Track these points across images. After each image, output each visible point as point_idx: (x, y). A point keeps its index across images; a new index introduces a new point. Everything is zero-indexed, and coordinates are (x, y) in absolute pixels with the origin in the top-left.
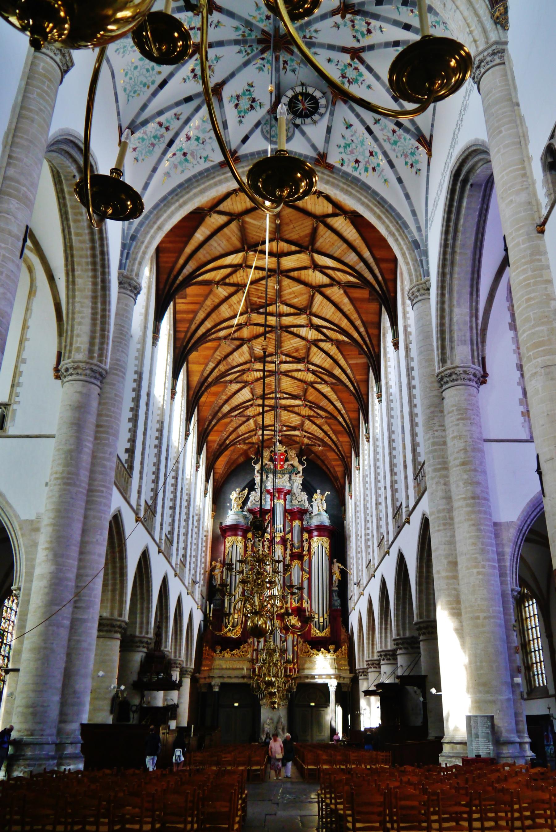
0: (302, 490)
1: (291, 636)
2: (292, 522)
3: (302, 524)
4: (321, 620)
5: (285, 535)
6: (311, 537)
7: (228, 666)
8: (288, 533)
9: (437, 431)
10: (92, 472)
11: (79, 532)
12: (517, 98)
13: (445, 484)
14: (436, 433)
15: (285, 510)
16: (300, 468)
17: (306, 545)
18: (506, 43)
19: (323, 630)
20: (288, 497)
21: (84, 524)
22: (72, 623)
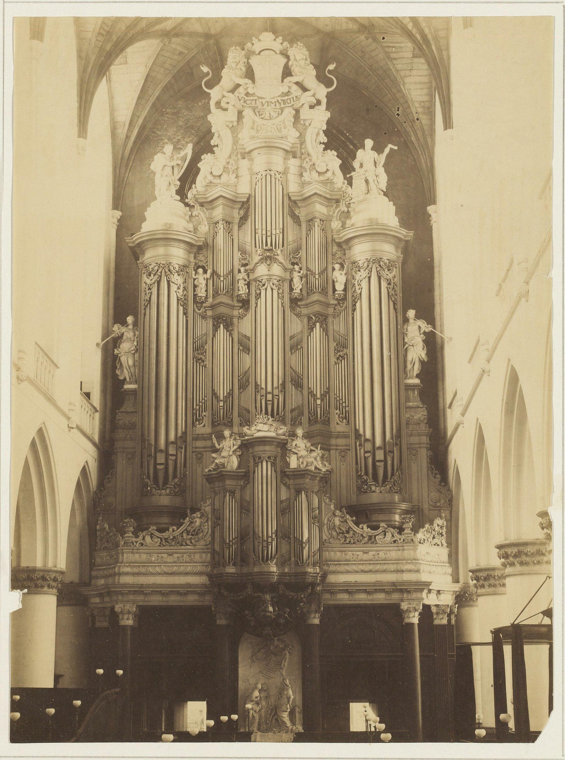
0: (327, 146)
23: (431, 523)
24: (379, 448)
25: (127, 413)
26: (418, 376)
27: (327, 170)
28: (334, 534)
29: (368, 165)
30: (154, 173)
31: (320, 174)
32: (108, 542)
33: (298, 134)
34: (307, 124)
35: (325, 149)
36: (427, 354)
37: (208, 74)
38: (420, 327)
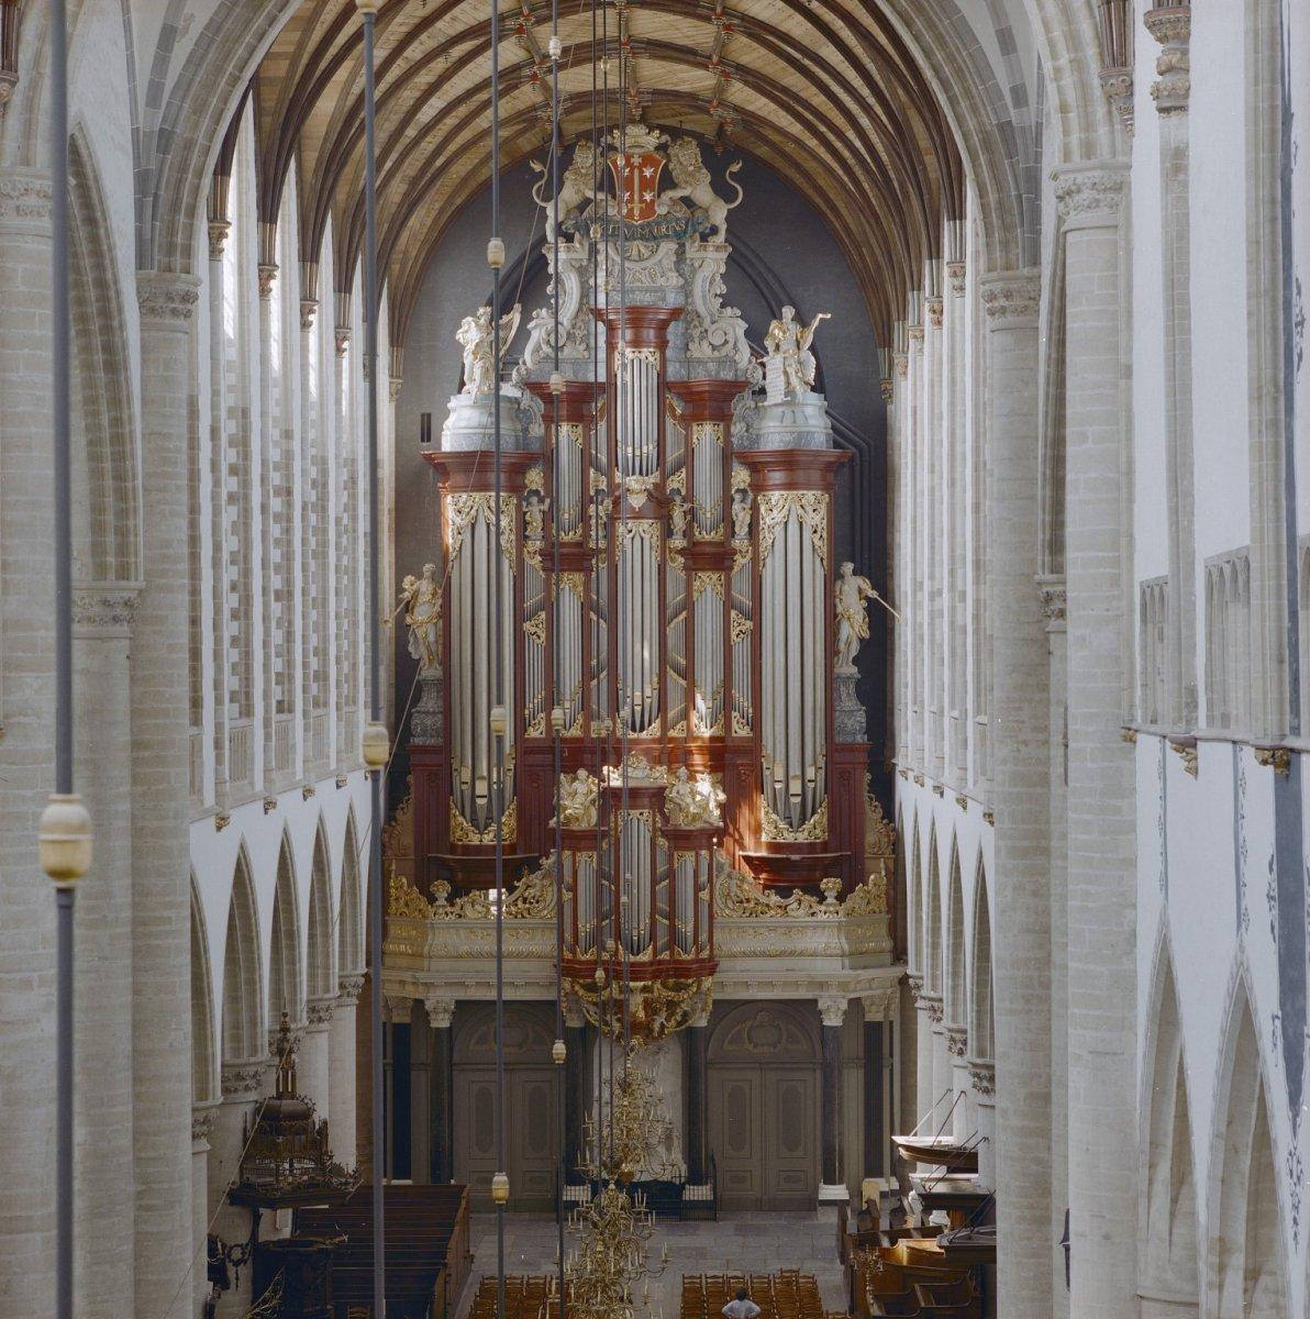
1: (690, 857)
2: (688, 428)
3: (728, 433)
4: (796, 787)
5: (664, 478)
6: (758, 487)
7: (476, 948)
8: (677, 469)
9: (1026, 743)
10: (137, 872)
11: (125, 1033)
12: (1130, 349)
13: (1035, 894)
14: (1022, 747)
15: (664, 386)
16: (719, 213)
17: (741, 514)
18: (1129, 167)
19: (803, 820)
20: (674, 332)
21: (136, 1007)
22: (137, 1242)
23: (865, 883)
24: (795, 777)
25: (427, 713)
26: (855, 661)
27: (726, 342)
28: (730, 905)
29: (788, 346)
30: (461, 348)
31: (714, 348)
32: (407, 905)
33: (681, 281)
34: (696, 265)
35: (723, 306)
36: (869, 628)
37: (542, 172)
38: (860, 591)
